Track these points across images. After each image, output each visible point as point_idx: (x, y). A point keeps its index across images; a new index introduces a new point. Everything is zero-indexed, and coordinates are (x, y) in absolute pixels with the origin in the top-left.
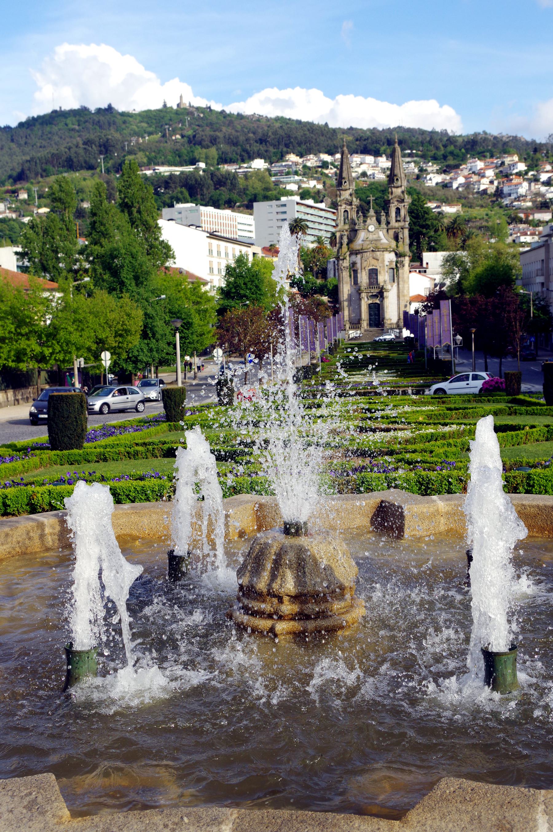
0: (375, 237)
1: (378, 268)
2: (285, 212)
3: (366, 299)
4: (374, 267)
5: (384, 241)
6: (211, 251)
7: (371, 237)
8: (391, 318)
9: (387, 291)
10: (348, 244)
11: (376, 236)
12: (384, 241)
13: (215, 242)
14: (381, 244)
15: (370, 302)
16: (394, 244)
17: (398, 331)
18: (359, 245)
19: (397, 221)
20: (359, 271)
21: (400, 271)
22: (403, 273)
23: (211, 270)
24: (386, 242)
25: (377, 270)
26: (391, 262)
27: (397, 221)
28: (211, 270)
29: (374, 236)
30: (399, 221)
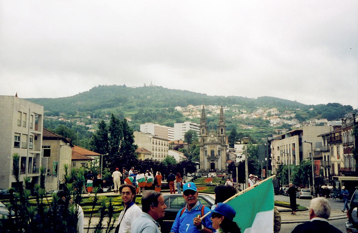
0: (213, 139)
1: (214, 150)
2: (185, 127)
6: (153, 143)
7: (212, 139)
8: (219, 168)
10: (204, 142)
13: (155, 140)
14: (216, 142)
15: (211, 162)
16: (220, 142)
17: (221, 174)
18: (208, 142)
19: (221, 134)
20: (208, 151)
23: (153, 149)
25: (214, 151)
26: (219, 148)
27: (221, 134)
28: (153, 149)
30: (223, 134)
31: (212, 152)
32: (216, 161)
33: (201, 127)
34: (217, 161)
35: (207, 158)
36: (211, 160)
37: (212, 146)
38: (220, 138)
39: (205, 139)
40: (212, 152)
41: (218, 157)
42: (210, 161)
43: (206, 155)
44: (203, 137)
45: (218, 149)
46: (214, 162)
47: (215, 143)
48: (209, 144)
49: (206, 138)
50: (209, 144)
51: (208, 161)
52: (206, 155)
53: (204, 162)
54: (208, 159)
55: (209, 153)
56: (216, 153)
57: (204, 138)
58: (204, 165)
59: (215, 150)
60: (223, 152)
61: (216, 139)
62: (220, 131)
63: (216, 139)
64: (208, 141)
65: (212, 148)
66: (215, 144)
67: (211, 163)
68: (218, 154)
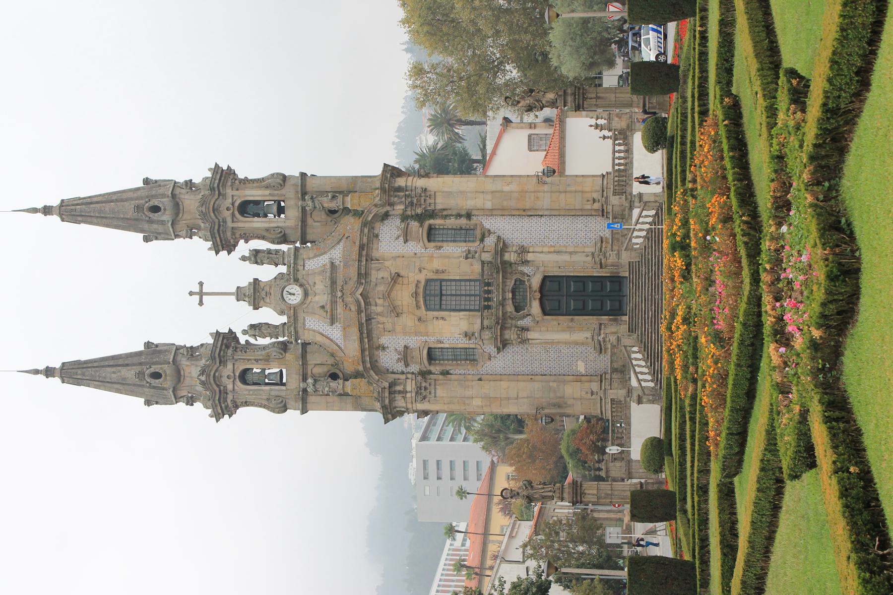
1: (422, 277)
3: (526, 322)
4: (421, 290)
5: (336, 253)
7: (321, 297)
9: (502, 247)
11: (318, 279)
12: (336, 253)
14: (346, 266)
17: (636, 212)
18: (345, 337)
19: (281, 210)
20: (432, 341)
21: (440, 203)
22: (449, 194)
24: (340, 246)
25: (428, 281)
29: (320, 287)
31: (436, 295)
32: (526, 262)
33: (223, 392)
34: (523, 250)
35: (491, 349)
36: (510, 308)
37: (387, 296)
38: (315, 227)
39: (331, 361)
40: (436, 295)
41: (490, 241)
42: (526, 322)
43: (468, 356)
44: (305, 379)
45: (414, 247)
46: (536, 282)
47: (353, 273)
48: (366, 331)
49: (314, 359)
50: (366, 331)
51: (524, 341)
52: (468, 356)
53: (532, 376)
54: (503, 344)
55: (452, 328)
56: (453, 260)
57: (318, 370)
58: (561, 377)
59: (414, 277)
60: (439, 200)
61: (324, 260)
62: (257, 223)
63: (324, 260)
64: (335, 333)
65: (404, 296)
66: (363, 276)
67: (545, 312)
68: (454, 249)
